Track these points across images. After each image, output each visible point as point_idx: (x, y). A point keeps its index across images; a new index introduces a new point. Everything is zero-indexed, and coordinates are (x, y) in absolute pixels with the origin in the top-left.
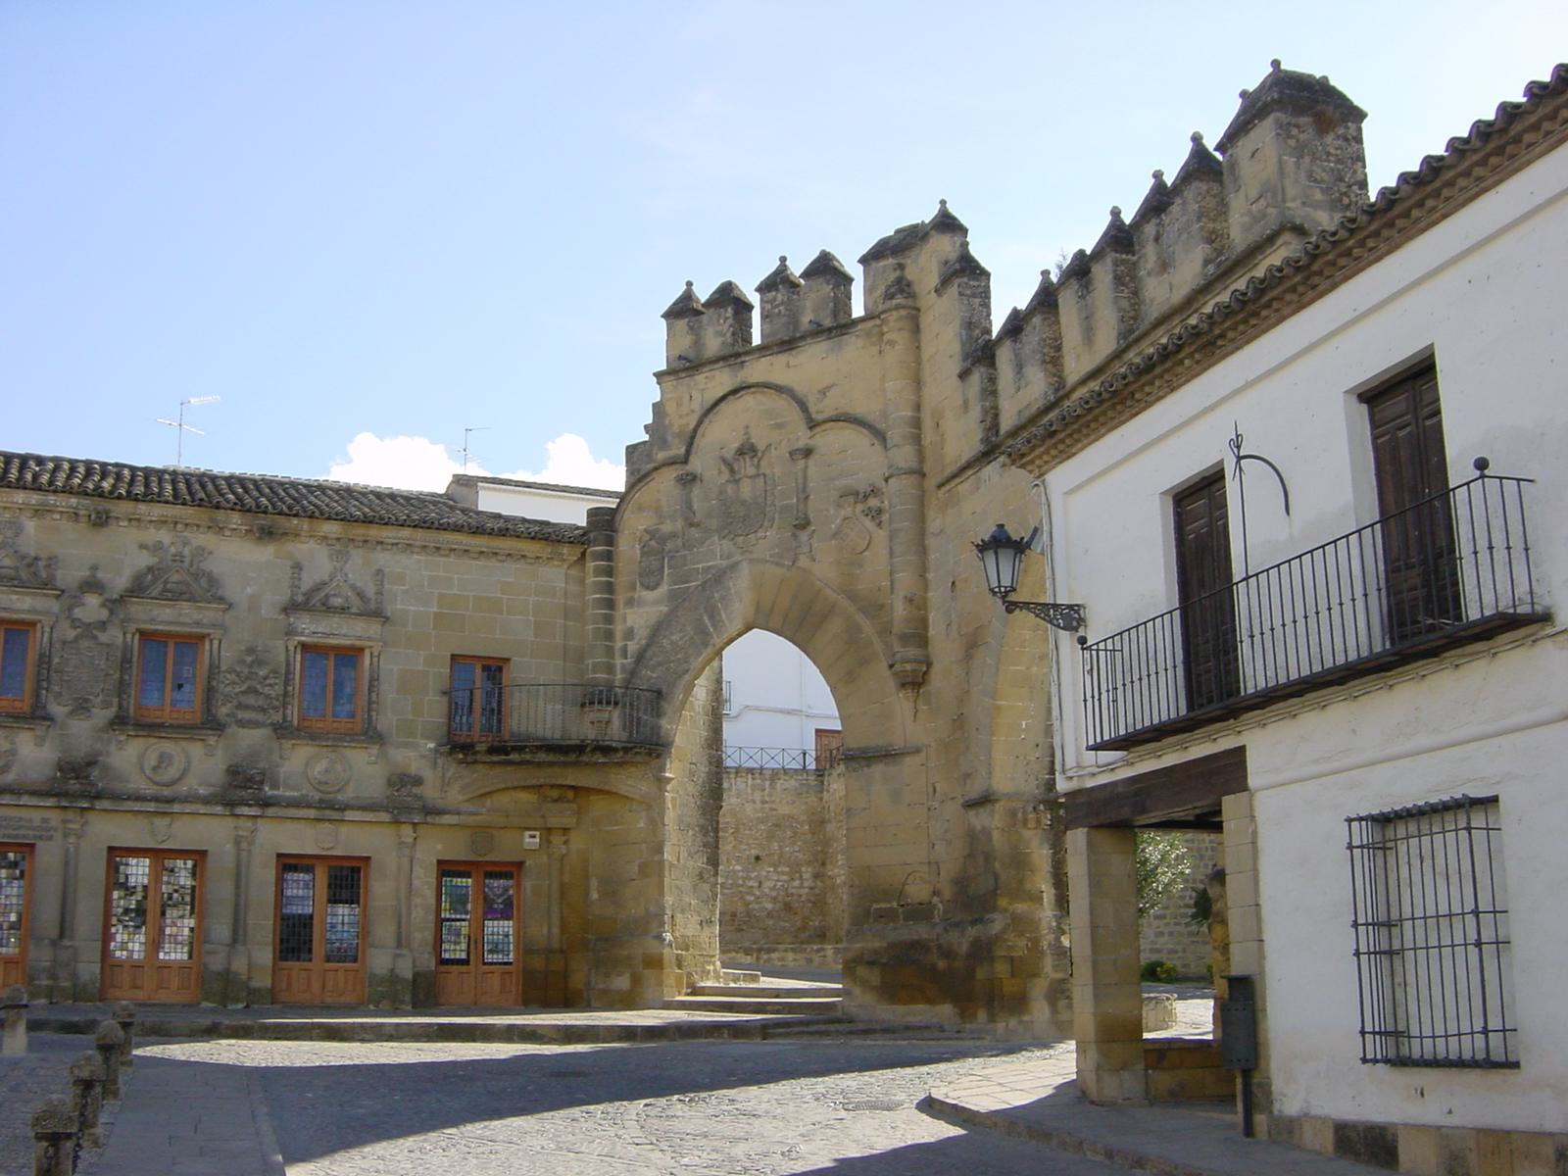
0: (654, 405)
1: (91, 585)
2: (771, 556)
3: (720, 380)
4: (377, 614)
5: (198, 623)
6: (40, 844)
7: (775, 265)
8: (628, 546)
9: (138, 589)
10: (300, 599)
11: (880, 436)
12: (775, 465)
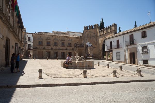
1: (59, 40)
3: (87, 31)
4: (71, 41)
8: (82, 38)
9: (61, 40)
11: (94, 34)
12: (90, 35)
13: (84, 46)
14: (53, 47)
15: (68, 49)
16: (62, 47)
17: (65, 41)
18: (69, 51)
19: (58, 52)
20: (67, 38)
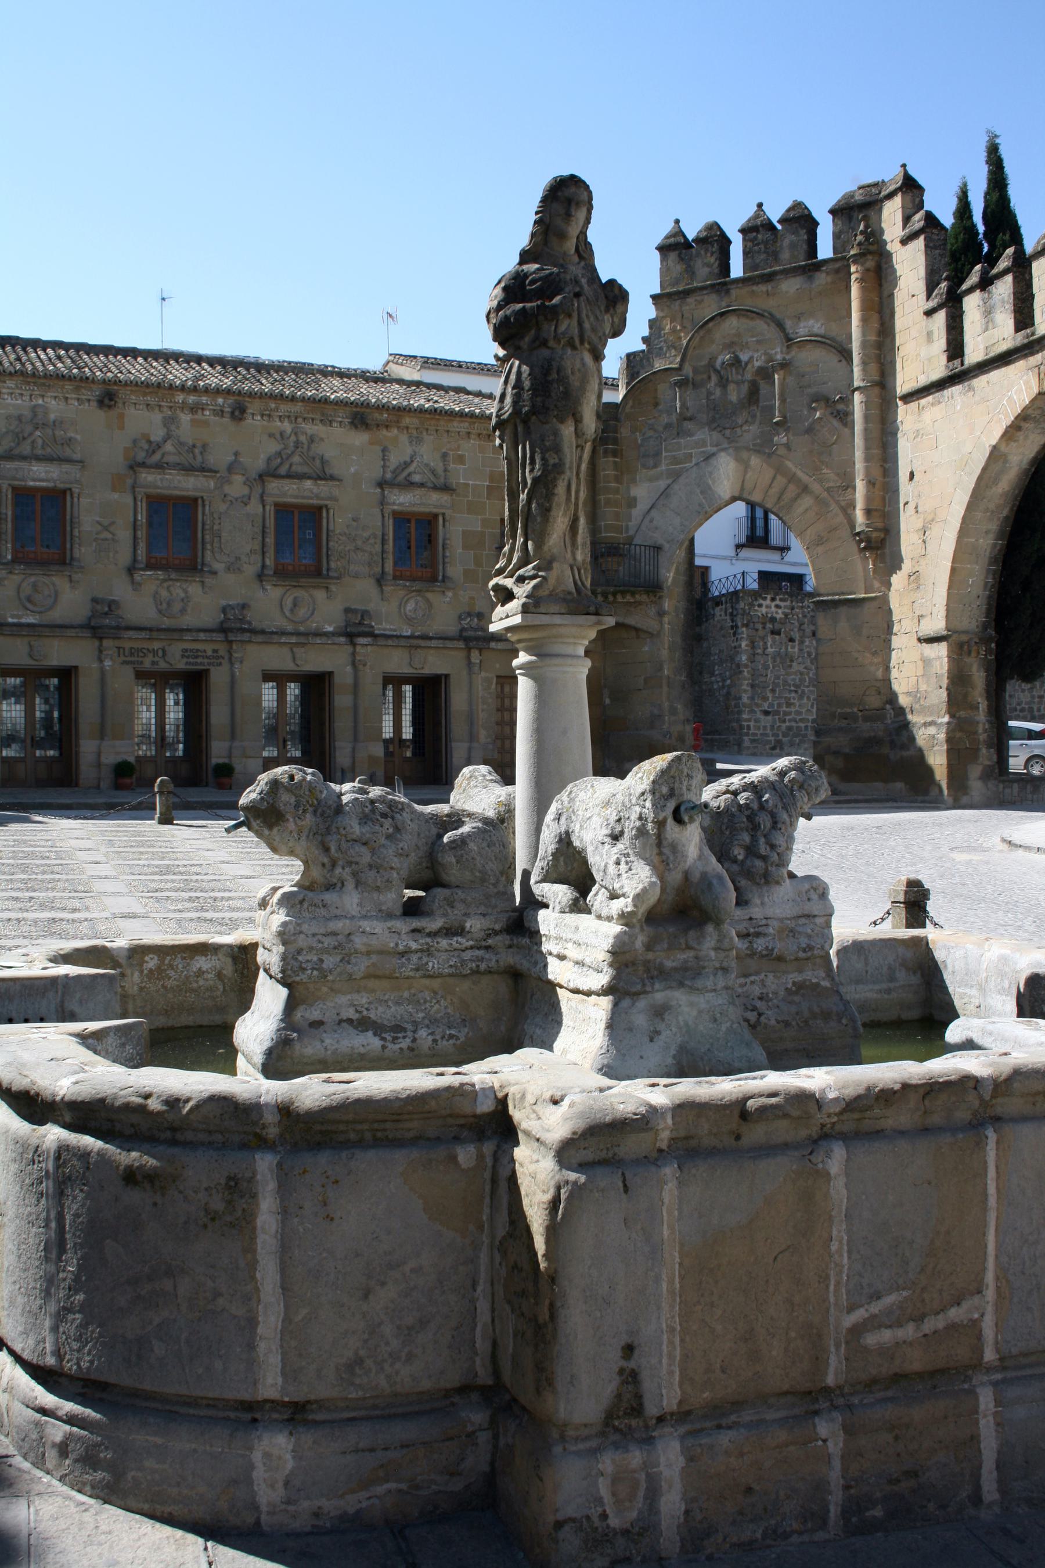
0: (650, 321)
2: (754, 445)
3: (710, 306)
4: (446, 488)
5: (317, 496)
6: (212, 669)
7: (751, 211)
10: (389, 476)
13: (670, 575)
14: (120, 590)
15: (379, 628)
16: (273, 592)
17: (323, 476)
18: (398, 662)
19: (218, 677)
20: (360, 438)
